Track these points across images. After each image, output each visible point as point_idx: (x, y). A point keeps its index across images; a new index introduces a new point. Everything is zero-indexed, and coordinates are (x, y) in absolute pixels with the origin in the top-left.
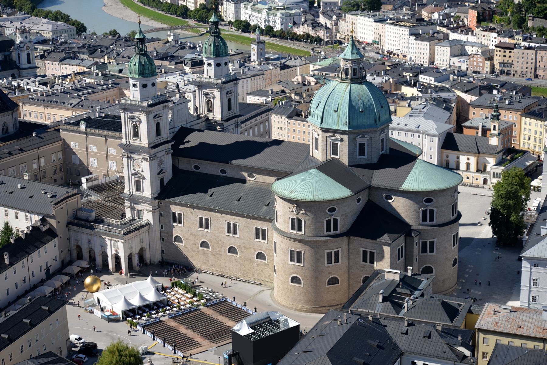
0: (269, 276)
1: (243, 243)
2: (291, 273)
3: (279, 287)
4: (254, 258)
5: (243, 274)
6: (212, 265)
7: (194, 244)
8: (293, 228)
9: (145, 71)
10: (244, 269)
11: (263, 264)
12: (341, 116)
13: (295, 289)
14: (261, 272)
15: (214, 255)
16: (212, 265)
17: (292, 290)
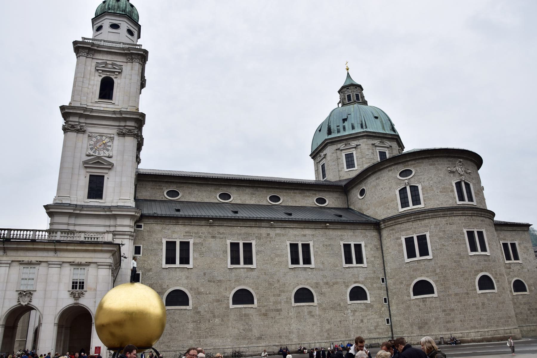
0: (376, 327)
1: (324, 277)
2: (477, 272)
3: (453, 310)
4: (345, 300)
5: (327, 338)
6: (260, 338)
7: (218, 301)
8: (461, 198)
9: (133, 15)
10: (328, 327)
11: (364, 307)
12: (384, 122)
13: (488, 300)
14: (361, 325)
15: (265, 315)
16: (260, 338)
17: (483, 304)
